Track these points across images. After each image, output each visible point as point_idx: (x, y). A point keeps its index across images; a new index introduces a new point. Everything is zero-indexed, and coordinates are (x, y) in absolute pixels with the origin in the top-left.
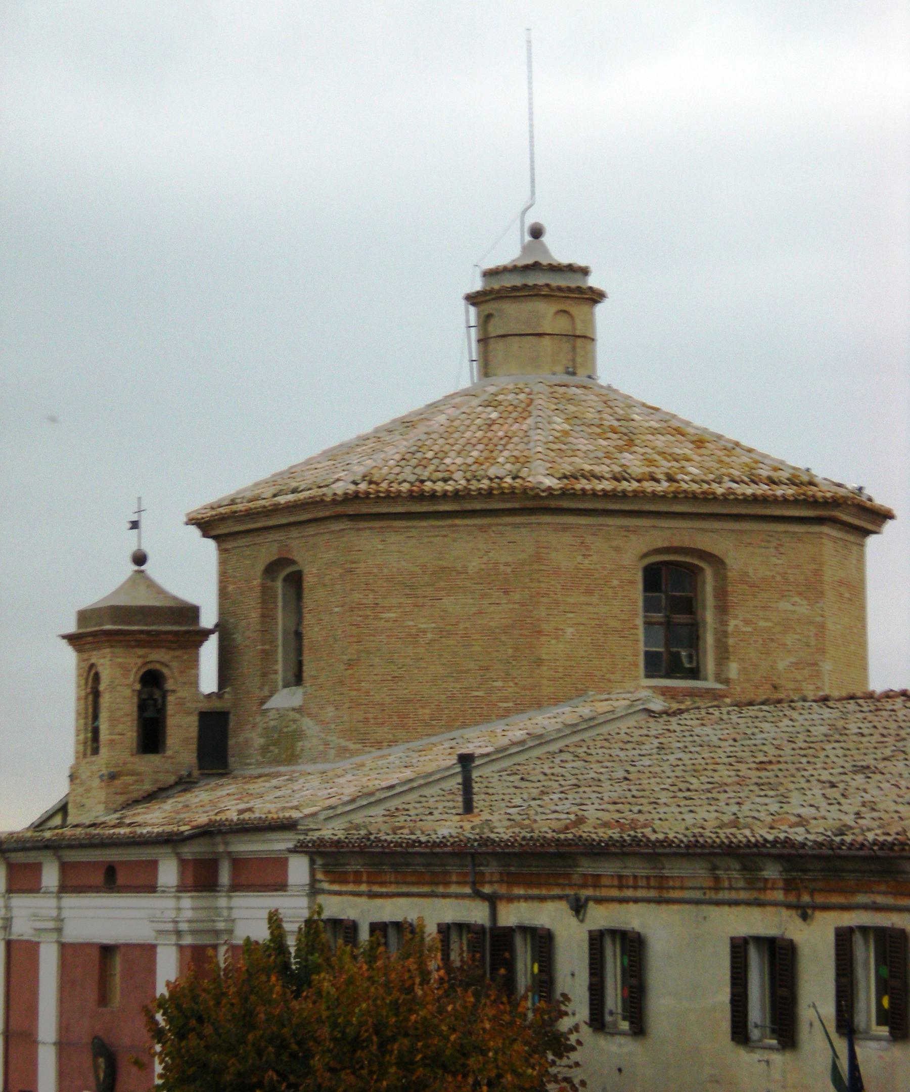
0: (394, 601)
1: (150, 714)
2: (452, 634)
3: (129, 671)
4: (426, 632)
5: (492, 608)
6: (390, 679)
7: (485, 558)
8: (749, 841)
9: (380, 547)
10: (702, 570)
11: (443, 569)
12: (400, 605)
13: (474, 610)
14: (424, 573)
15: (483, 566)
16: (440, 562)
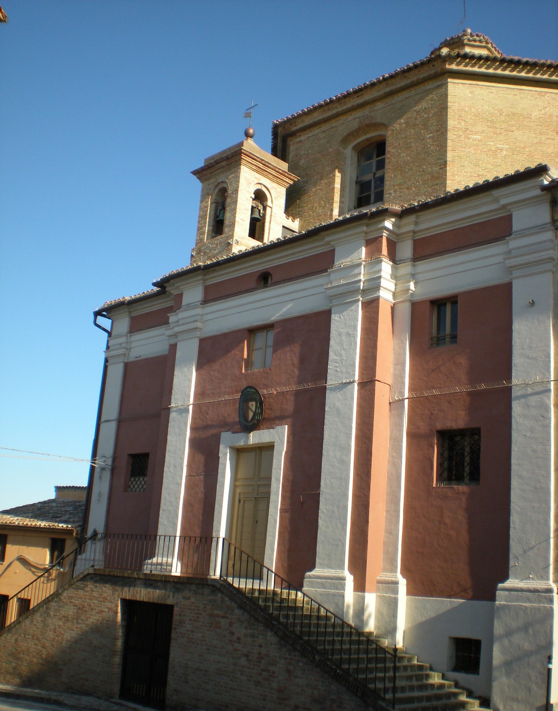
0: (480, 129)
1: (256, 215)
2: (521, 153)
3: (250, 184)
4: (502, 150)
5: (549, 141)
6: (476, 175)
7: (543, 112)
8: (80, 526)
9: (470, 95)
10: (394, 300)
11: (514, 114)
12: (483, 132)
13: (536, 140)
14: (501, 114)
15: (541, 116)
16: (512, 110)
